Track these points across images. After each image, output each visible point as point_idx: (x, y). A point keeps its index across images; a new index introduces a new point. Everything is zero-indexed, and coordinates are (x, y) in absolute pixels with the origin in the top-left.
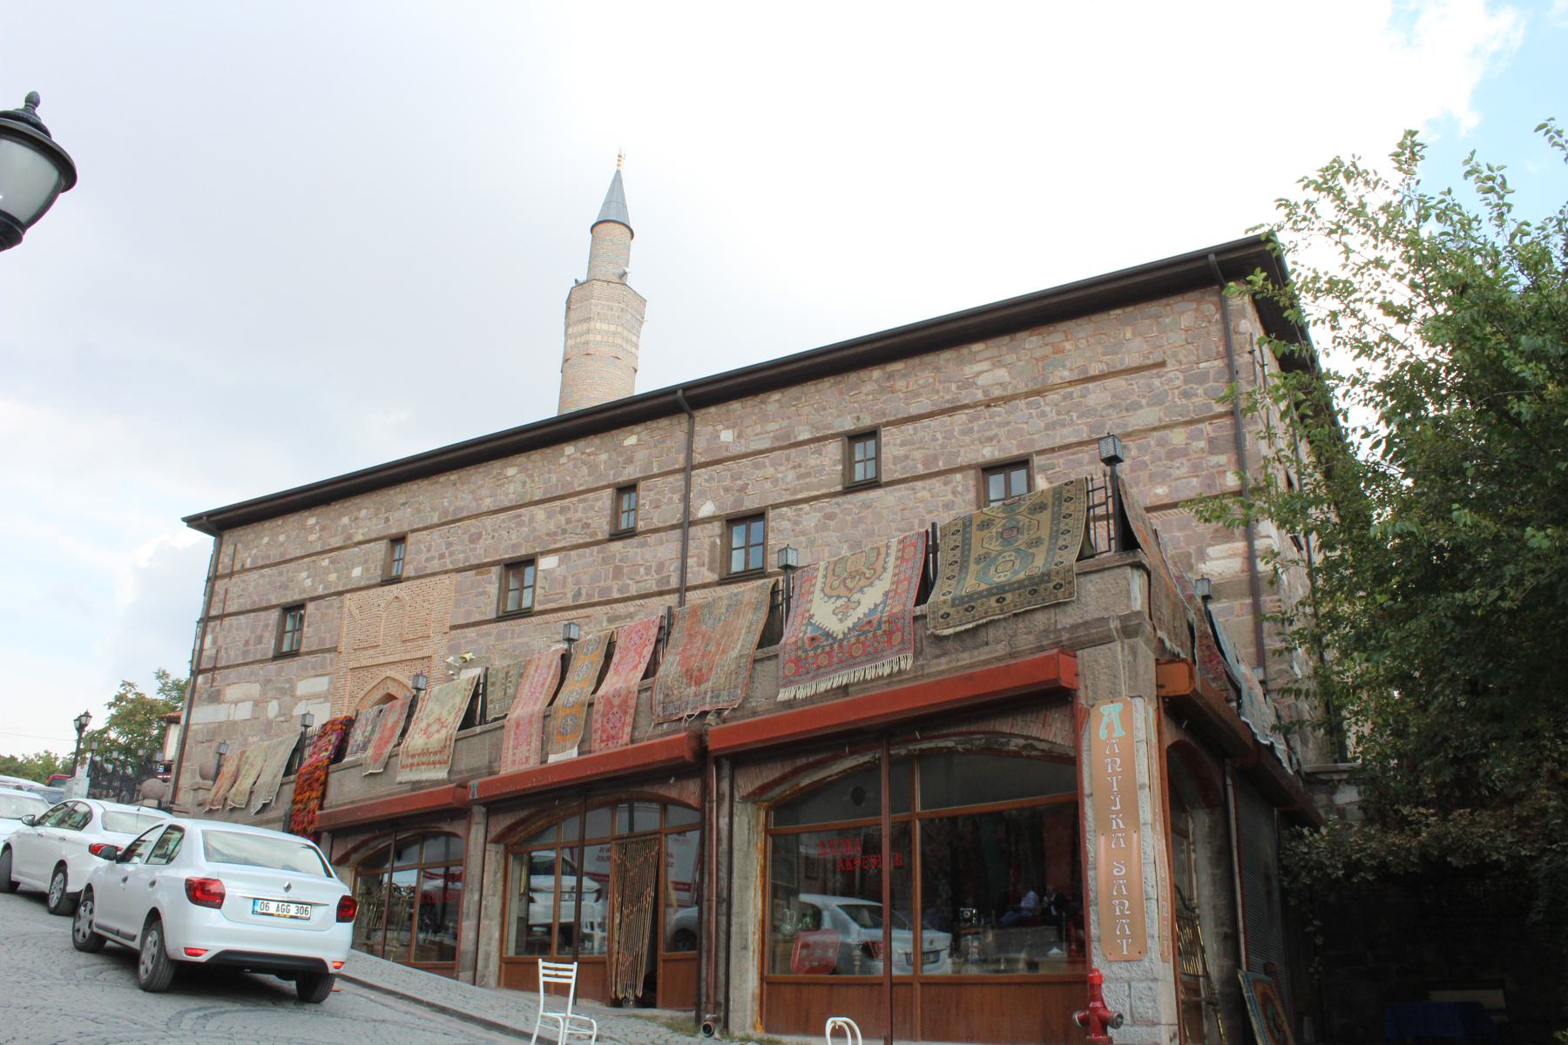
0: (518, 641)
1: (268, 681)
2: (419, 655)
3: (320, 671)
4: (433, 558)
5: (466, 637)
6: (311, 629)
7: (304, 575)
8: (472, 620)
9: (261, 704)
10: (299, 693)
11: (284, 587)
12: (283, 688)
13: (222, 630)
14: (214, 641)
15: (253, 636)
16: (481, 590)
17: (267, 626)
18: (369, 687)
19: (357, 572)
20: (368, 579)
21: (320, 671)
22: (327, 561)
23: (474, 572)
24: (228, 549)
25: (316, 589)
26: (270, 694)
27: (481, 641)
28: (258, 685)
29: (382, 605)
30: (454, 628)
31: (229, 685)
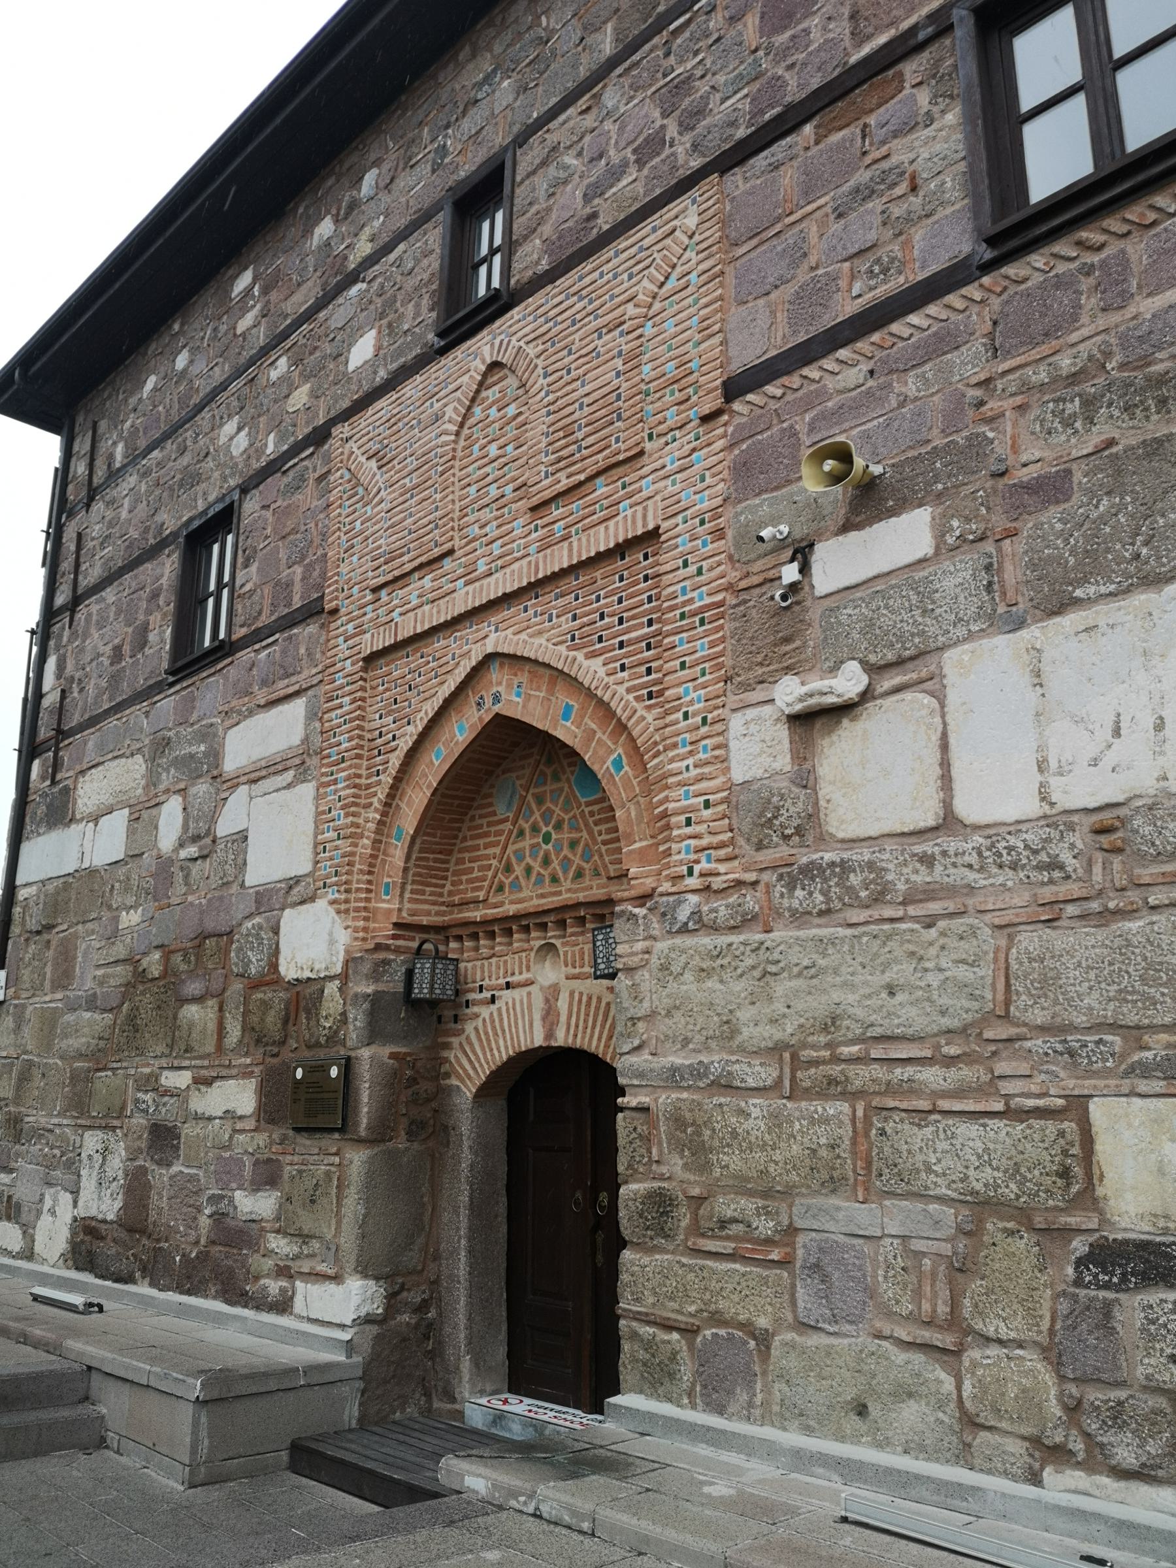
0: (1148, 306)
1: (161, 745)
2: (603, 539)
3: (282, 687)
4: (615, 174)
5: (822, 395)
6: (254, 568)
7: (230, 427)
8: (846, 307)
9: (145, 815)
10: (231, 764)
11: (191, 479)
12: (192, 756)
13: (74, 636)
14: (61, 667)
15: (130, 630)
16: (862, 176)
17: (155, 595)
18: (430, 708)
19: (362, 351)
20: (400, 352)
21: (282, 687)
22: (283, 362)
23: (808, 129)
24: (82, 445)
25: (260, 451)
26: (166, 780)
27: (911, 385)
28: (139, 758)
29: (449, 412)
30: (733, 389)
31: (82, 772)
